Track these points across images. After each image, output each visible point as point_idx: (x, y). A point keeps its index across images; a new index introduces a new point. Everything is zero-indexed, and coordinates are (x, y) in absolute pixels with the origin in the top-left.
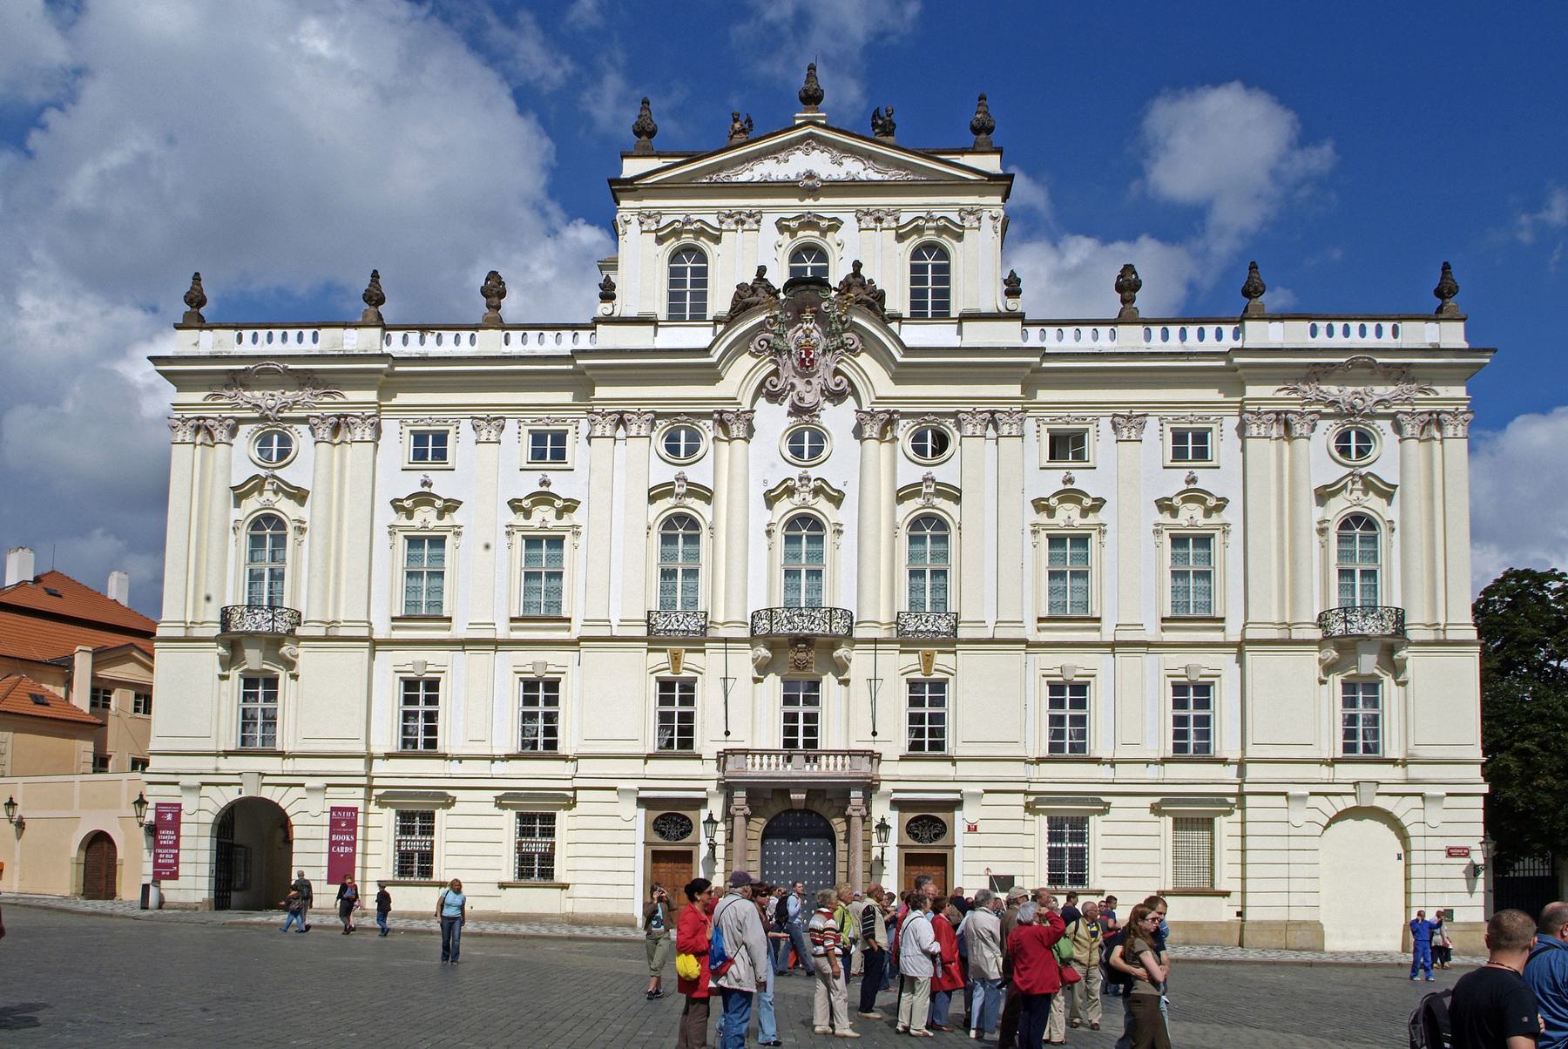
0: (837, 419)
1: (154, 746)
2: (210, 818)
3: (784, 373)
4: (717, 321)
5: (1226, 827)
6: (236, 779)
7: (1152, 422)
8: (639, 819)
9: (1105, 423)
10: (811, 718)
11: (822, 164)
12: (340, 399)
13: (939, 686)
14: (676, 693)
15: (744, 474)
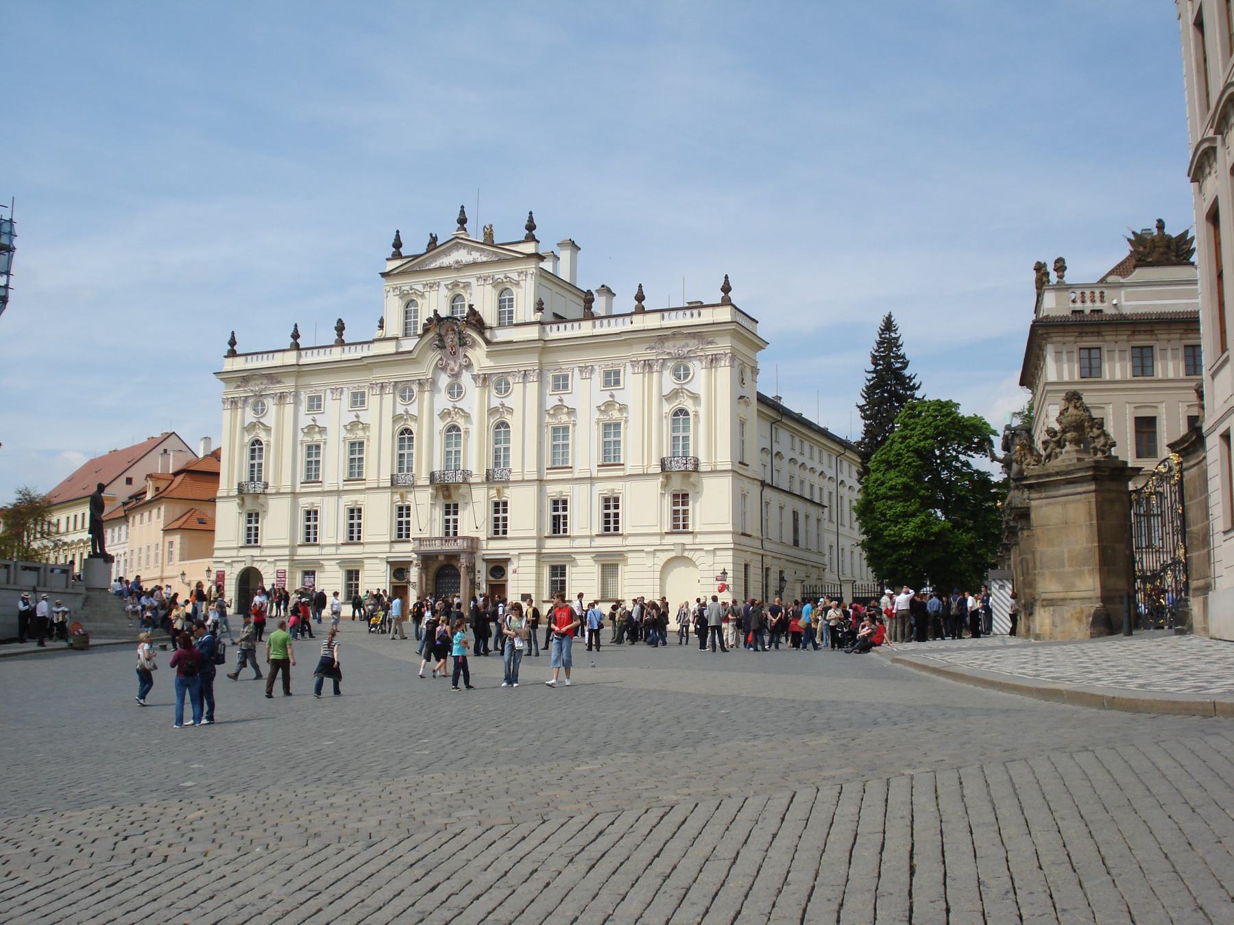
1: (216, 545)
2: (235, 576)
7: (596, 367)
9: (576, 370)
10: (456, 521)
11: (462, 256)
13: (505, 504)
14: (403, 511)
15: (428, 411)
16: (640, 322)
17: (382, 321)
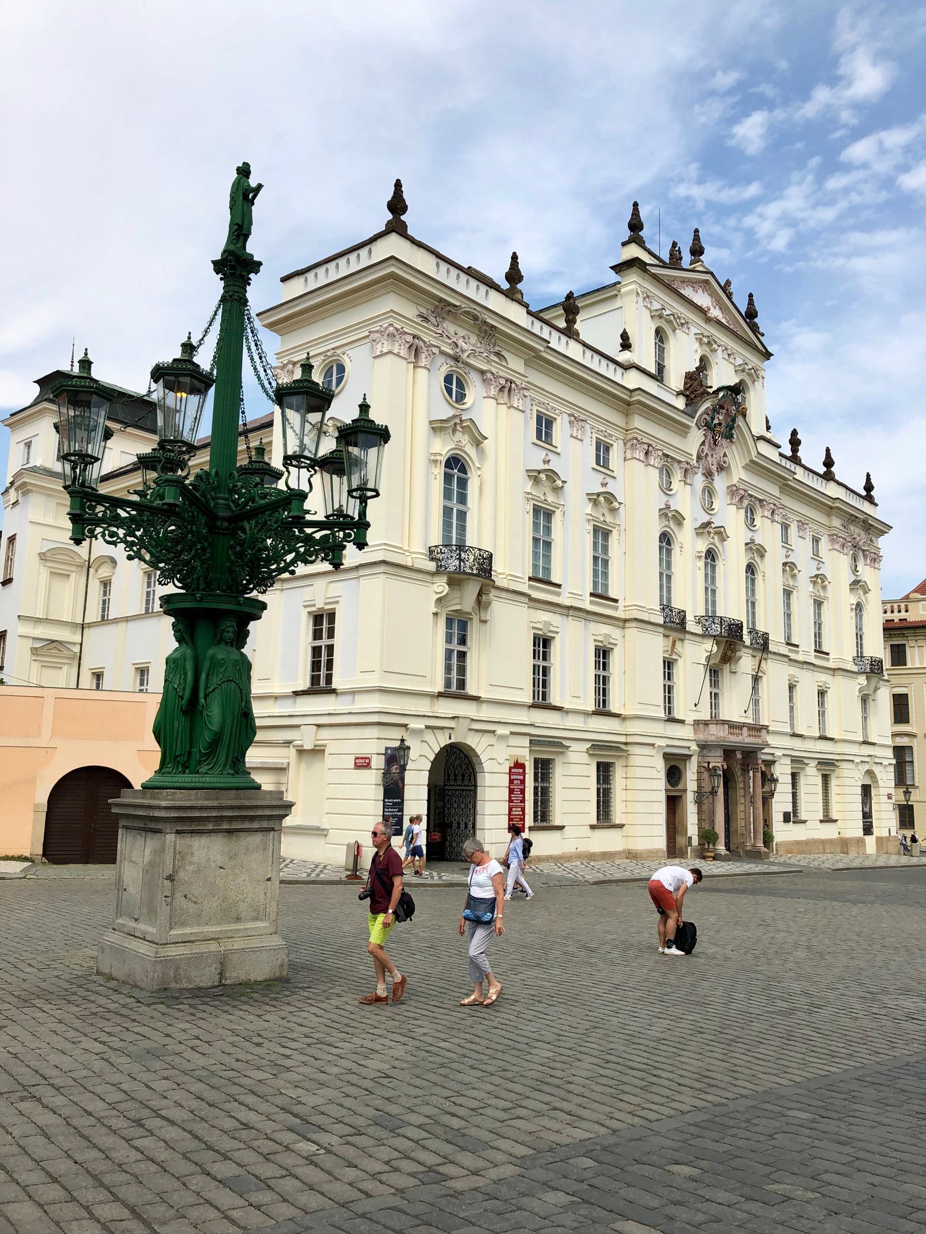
0: (720, 483)
3: (707, 444)
4: (679, 394)
6: (451, 724)
8: (659, 767)
12: (504, 364)
16: (832, 490)
17: (625, 336)
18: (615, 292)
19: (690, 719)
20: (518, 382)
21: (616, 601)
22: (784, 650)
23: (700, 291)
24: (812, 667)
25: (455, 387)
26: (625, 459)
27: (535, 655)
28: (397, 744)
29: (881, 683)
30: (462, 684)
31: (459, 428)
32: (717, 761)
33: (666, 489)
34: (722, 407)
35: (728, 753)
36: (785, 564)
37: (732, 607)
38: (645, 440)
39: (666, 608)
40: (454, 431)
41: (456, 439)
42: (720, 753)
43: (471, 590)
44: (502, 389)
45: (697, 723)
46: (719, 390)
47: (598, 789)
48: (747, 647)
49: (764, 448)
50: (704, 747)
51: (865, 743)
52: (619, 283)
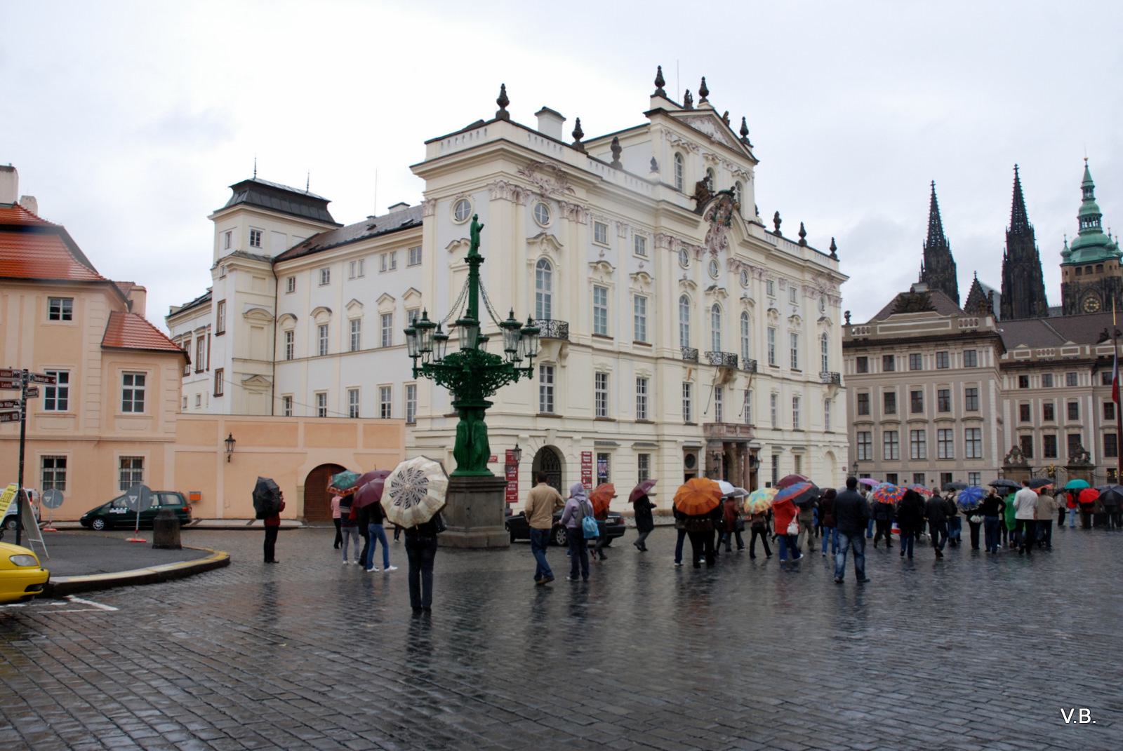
0: (722, 256)
4: (692, 198)
5: (804, 460)
8: (680, 456)
17: (653, 162)
18: (646, 130)
19: (701, 424)
20: (582, 205)
21: (650, 346)
22: (768, 371)
23: (706, 123)
24: (788, 382)
25: (542, 216)
26: (655, 247)
27: (597, 385)
28: (513, 447)
29: (840, 389)
30: (550, 408)
31: (545, 241)
32: (719, 450)
33: (684, 263)
34: (721, 205)
35: (727, 444)
36: (769, 310)
37: (731, 345)
38: (668, 234)
39: (684, 348)
40: (542, 243)
41: (543, 248)
42: (721, 444)
43: (556, 347)
44: (572, 211)
45: (706, 425)
46: (721, 193)
47: (639, 472)
48: (741, 371)
49: (755, 231)
50: (710, 441)
51: (826, 432)
52: (649, 124)
